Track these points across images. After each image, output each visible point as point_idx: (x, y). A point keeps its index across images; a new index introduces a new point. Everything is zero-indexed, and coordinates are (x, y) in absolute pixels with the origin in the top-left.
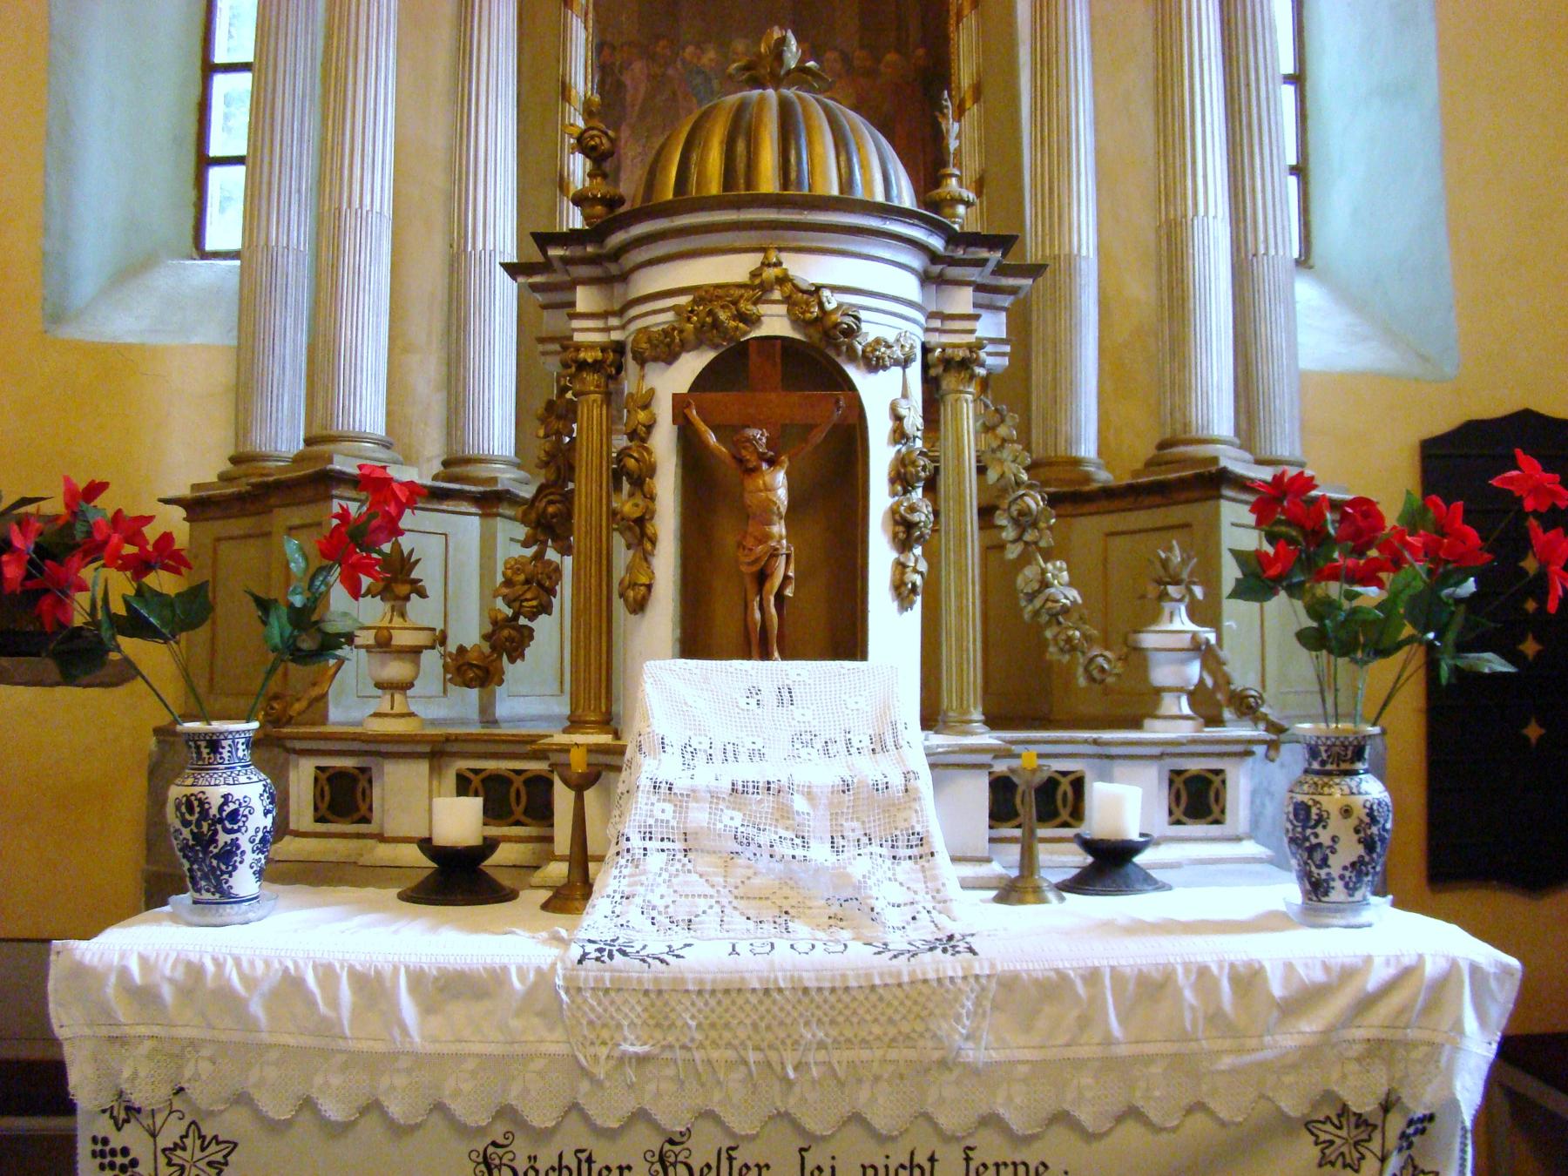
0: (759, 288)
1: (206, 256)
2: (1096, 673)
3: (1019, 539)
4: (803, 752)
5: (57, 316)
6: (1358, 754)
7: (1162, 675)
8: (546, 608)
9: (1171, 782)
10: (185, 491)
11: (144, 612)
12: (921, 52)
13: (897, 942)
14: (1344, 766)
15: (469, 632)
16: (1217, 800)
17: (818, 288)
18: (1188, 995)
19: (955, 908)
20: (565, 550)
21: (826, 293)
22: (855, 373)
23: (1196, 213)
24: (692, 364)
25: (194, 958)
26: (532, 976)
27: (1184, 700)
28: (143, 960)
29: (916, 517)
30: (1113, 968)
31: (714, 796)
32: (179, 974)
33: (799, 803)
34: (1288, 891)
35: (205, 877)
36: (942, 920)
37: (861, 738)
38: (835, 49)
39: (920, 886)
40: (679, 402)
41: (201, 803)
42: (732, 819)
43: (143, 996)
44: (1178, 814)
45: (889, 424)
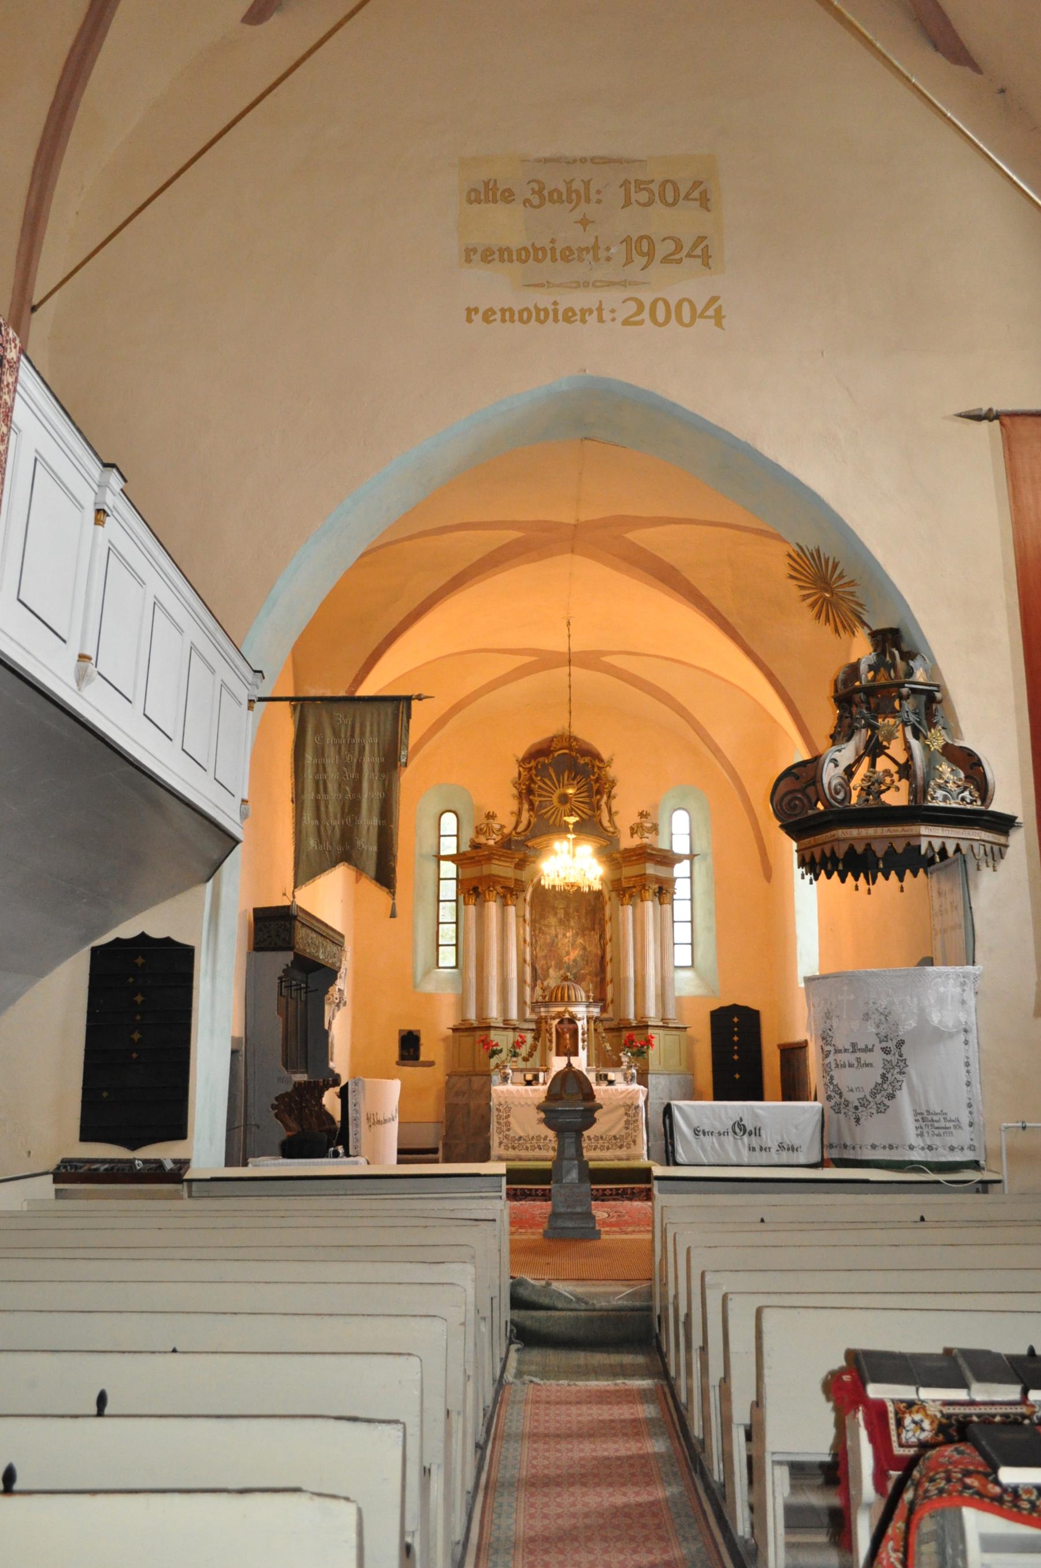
0: (565, 1012)
1: (439, 968)
5: (415, 987)
10: (451, 1026)
22: (577, 1022)
24: (557, 1021)
43: (502, 1092)
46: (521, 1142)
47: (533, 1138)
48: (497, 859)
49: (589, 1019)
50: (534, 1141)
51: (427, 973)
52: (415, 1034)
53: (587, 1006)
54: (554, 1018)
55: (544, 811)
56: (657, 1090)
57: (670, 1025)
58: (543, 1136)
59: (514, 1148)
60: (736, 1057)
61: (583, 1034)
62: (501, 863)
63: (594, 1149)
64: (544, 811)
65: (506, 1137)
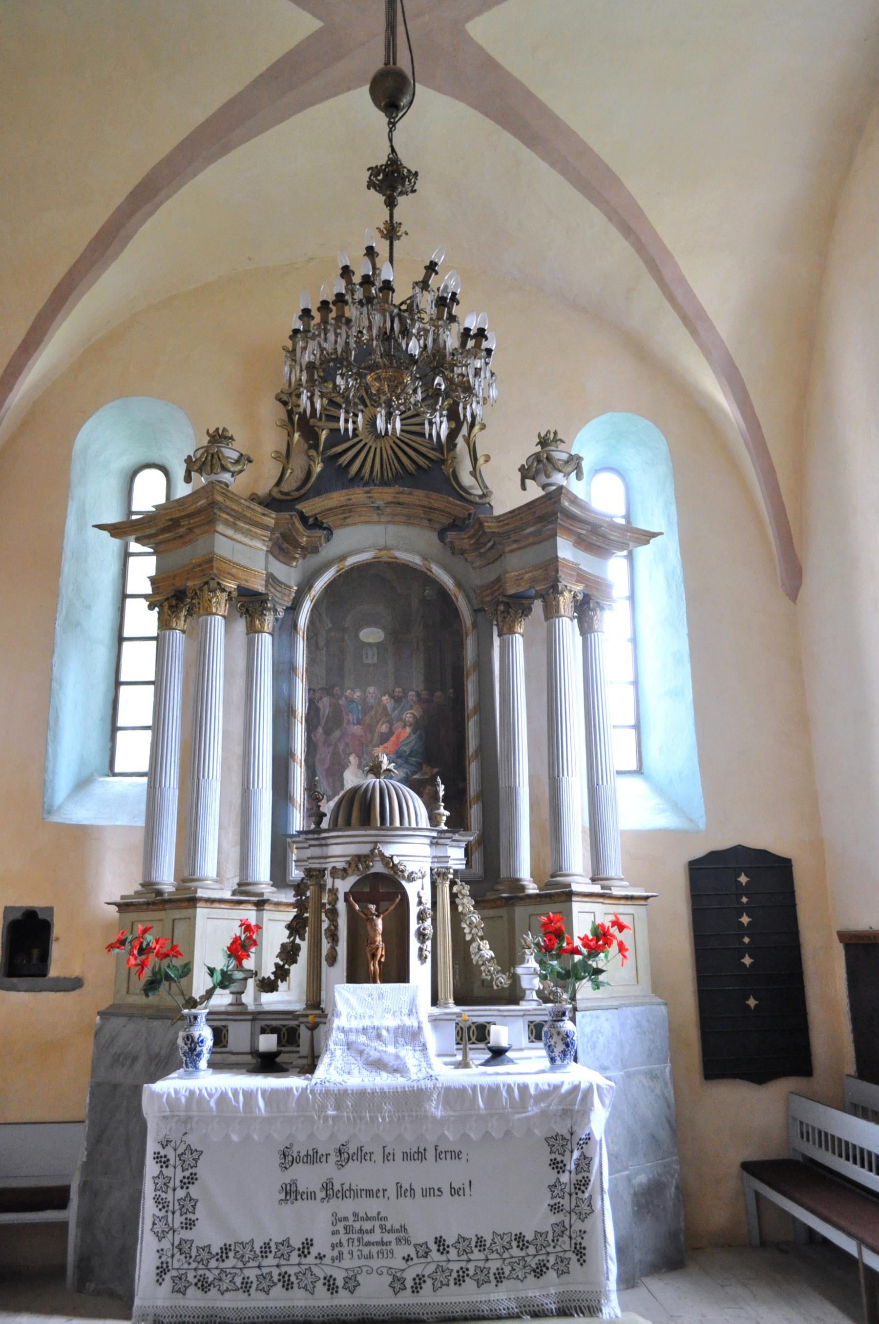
2: (499, 984)
3: (470, 932)
4: (386, 1015)
6: (564, 1014)
7: (525, 983)
8: (295, 962)
9: (529, 1026)
10: (117, 899)
11: (170, 973)
12: (451, 691)
13: (414, 1077)
14: (559, 1018)
15: (268, 971)
16: (532, 1030)
17: (392, 856)
18: (504, 1093)
19: (434, 1067)
20: (303, 939)
21: (395, 858)
22: (404, 883)
23: (563, 775)
24: (352, 880)
25: (192, 1088)
26: (300, 1090)
27: (534, 993)
28: (176, 1091)
29: (426, 932)
30: (480, 1085)
31: (357, 1031)
32: (187, 1093)
33: (384, 1033)
34: (547, 1063)
35: (191, 1063)
36: (429, 1070)
37: (405, 1011)
38: (412, 690)
39: (422, 1060)
40: (346, 894)
41: (192, 1037)
42: (362, 1039)
44: (532, 1038)
45: (417, 900)
46: (231, 1262)
47: (266, 1249)
48: (227, 523)
49: (437, 877)
50: (270, 1261)
51: (83, 784)
52: (41, 916)
53: (434, 843)
54: (344, 873)
55: (339, 449)
56: (594, 1047)
57: (616, 892)
58: (296, 1243)
59: (204, 1286)
60: (747, 961)
61: (421, 917)
62: (239, 537)
63: (459, 1281)
64: (339, 449)
65: (182, 1248)
